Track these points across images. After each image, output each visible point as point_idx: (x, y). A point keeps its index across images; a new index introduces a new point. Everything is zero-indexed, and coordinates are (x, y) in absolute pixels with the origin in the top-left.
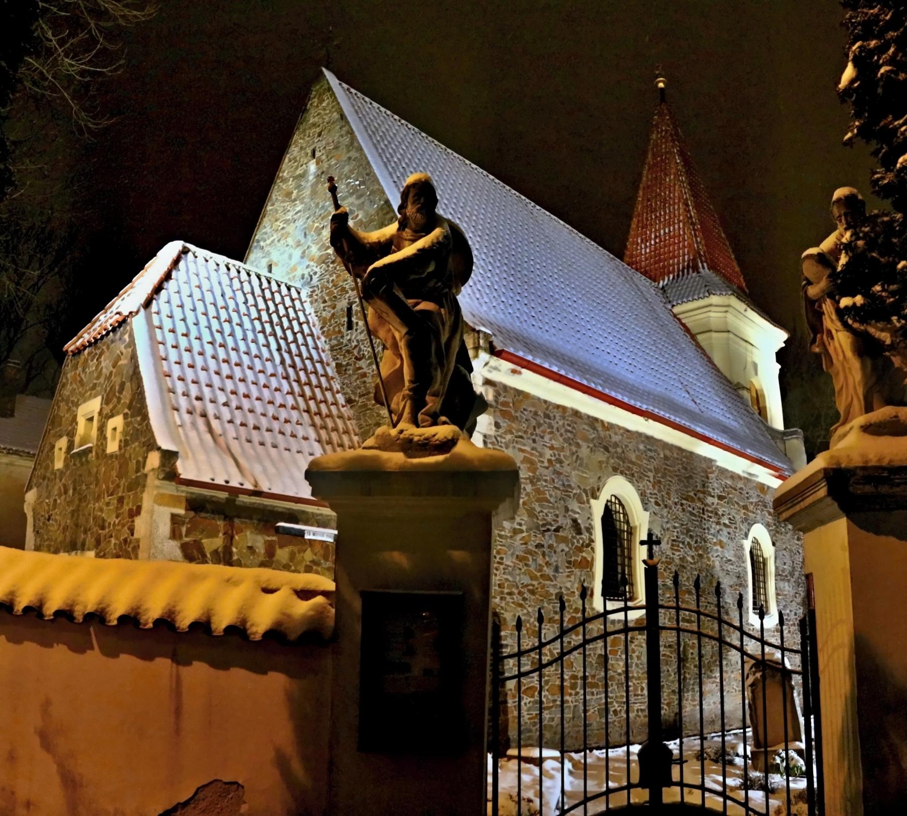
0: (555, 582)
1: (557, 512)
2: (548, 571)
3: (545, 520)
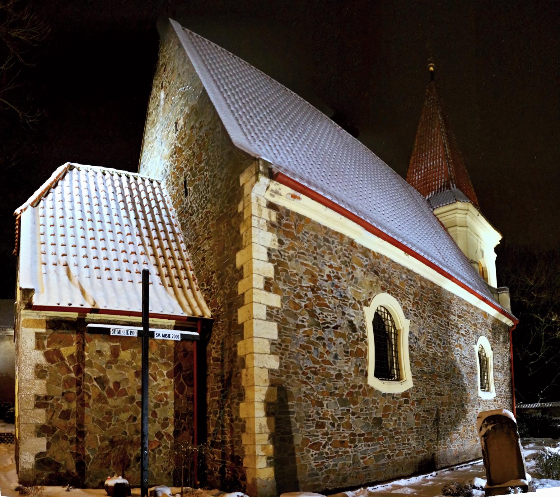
0: (334, 366)
1: (336, 316)
2: (330, 358)
3: (325, 320)
